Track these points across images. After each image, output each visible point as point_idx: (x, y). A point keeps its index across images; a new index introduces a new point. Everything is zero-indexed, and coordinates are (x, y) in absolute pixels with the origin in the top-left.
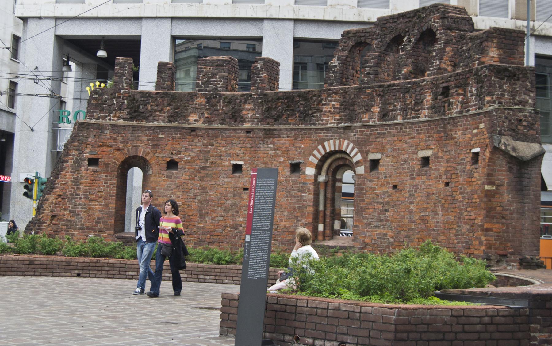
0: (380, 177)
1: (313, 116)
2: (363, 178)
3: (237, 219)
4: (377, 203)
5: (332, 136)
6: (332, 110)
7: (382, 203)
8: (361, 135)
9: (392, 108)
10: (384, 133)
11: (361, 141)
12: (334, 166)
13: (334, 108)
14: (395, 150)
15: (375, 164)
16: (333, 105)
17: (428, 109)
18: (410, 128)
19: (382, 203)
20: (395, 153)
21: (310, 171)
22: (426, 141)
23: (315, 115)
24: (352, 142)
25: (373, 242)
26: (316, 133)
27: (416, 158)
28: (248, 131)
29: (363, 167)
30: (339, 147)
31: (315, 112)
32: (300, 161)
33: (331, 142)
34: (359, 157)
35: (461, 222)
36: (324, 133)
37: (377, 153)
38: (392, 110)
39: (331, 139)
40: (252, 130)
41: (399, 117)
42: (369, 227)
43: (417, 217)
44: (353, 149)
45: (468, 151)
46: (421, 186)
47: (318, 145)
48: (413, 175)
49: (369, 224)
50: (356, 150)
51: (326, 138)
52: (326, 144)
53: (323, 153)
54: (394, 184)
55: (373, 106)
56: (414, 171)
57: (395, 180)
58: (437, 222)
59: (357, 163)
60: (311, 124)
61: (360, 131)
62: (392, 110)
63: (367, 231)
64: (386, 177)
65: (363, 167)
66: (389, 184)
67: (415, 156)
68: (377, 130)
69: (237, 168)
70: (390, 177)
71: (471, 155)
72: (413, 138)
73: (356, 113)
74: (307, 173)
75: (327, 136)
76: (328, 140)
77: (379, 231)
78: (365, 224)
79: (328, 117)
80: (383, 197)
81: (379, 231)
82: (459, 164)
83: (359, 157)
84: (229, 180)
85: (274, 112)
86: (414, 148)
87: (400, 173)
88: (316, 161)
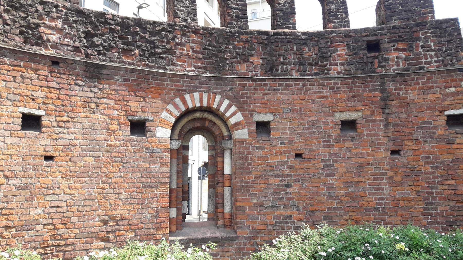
0: (274, 143)
1: (162, 58)
2: (246, 144)
3: (32, 211)
4: (272, 176)
5: (196, 87)
6: (191, 53)
7: (280, 176)
8: (241, 89)
9: (282, 60)
10: (277, 90)
11: (242, 97)
12: (188, 128)
13: (194, 51)
14: (294, 110)
15: (263, 127)
16: (192, 47)
17: (342, 64)
18: (319, 84)
19: (280, 176)
20: (296, 115)
21: (163, 133)
22: (348, 100)
23: (164, 56)
24: (228, 98)
25: (270, 227)
26: (171, 81)
27: (332, 122)
28: (55, 62)
29: (246, 130)
30: (208, 103)
31: (164, 53)
32: (147, 118)
33: (196, 95)
34: (239, 117)
35: (434, 198)
36: (185, 82)
37: (266, 113)
38: (283, 63)
39: (196, 91)
40: (64, 60)
41: (294, 72)
42: (261, 208)
43: (342, 193)
44: (229, 106)
45: (437, 113)
46: (344, 155)
47: (175, 98)
48: (329, 141)
49: (260, 205)
50: (233, 109)
51: (187, 89)
52: (187, 97)
53: (183, 109)
54: (297, 152)
55: (251, 56)
56: (330, 136)
57: (299, 147)
58: (383, 199)
59: (237, 124)
60: (159, 68)
61: (240, 85)
62: (283, 63)
63: (258, 213)
64: (282, 143)
65: (246, 130)
66: (289, 152)
67: (329, 119)
68: (266, 85)
69: (31, 122)
70: (290, 143)
71: (446, 118)
72: (324, 97)
73: (228, 62)
74: (158, 135)
75: (188, 86)
76: (191, 92)
77: (277, 213)
78: (255, 204)
79: (185, 61)
80: (281, 168)
81: (277, 213)
82: (421, 128)
83: (239, 117)
84: (16, 140)
85: (97, 41)
86: (327, 109)
87: (306, 139)
88: (173, 120)
